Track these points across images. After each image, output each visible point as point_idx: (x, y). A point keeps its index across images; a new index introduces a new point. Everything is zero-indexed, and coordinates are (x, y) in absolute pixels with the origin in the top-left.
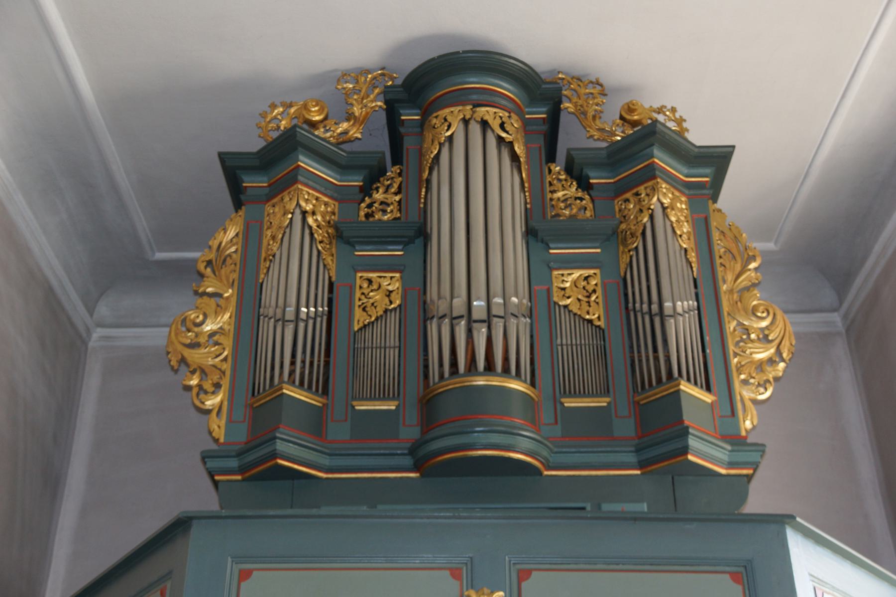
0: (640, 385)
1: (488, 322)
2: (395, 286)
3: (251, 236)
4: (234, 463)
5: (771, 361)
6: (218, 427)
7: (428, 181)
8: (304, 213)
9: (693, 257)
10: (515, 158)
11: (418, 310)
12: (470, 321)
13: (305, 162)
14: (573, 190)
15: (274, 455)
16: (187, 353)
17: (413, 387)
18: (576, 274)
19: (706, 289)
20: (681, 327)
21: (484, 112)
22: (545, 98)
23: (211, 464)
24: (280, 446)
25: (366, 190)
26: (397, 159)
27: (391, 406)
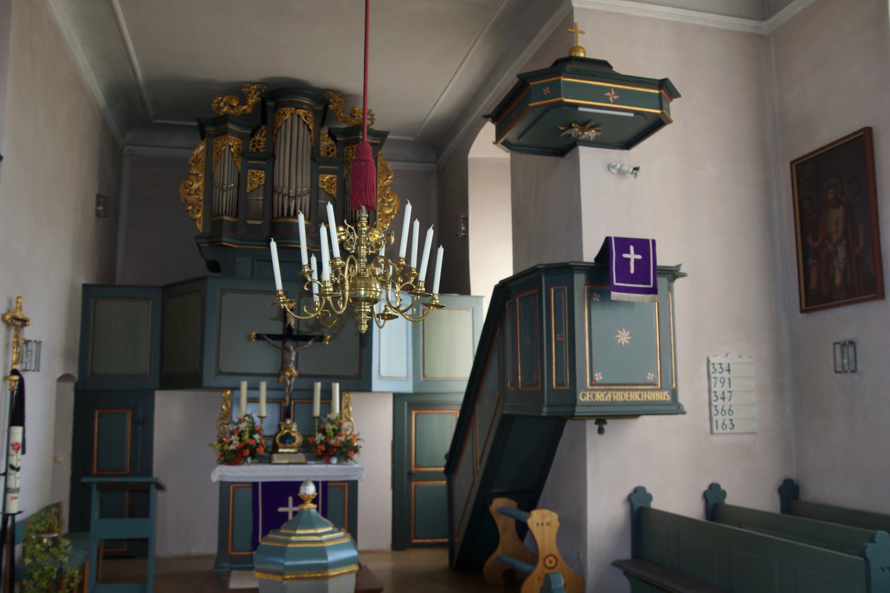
1: (295, 198)
2: (263, 175)
3: (209, 151)
4: (206, 241)
5: (391, 214)
6: (199, 226)
7: (276, 136)
8: (230, 147)
10: (309, 130)
11: (270, 188)
12: (289, 197)
13: (231, 126)
14: (331, 142)
15: (221, 241)
16: (188, 198)
18: (328, 177)
21: (301, 112)
22: (323, 103)
23: (199, 240)
24: (223, 239)
25: (252, 135)
26: (264, 121)
27: (259, 223)
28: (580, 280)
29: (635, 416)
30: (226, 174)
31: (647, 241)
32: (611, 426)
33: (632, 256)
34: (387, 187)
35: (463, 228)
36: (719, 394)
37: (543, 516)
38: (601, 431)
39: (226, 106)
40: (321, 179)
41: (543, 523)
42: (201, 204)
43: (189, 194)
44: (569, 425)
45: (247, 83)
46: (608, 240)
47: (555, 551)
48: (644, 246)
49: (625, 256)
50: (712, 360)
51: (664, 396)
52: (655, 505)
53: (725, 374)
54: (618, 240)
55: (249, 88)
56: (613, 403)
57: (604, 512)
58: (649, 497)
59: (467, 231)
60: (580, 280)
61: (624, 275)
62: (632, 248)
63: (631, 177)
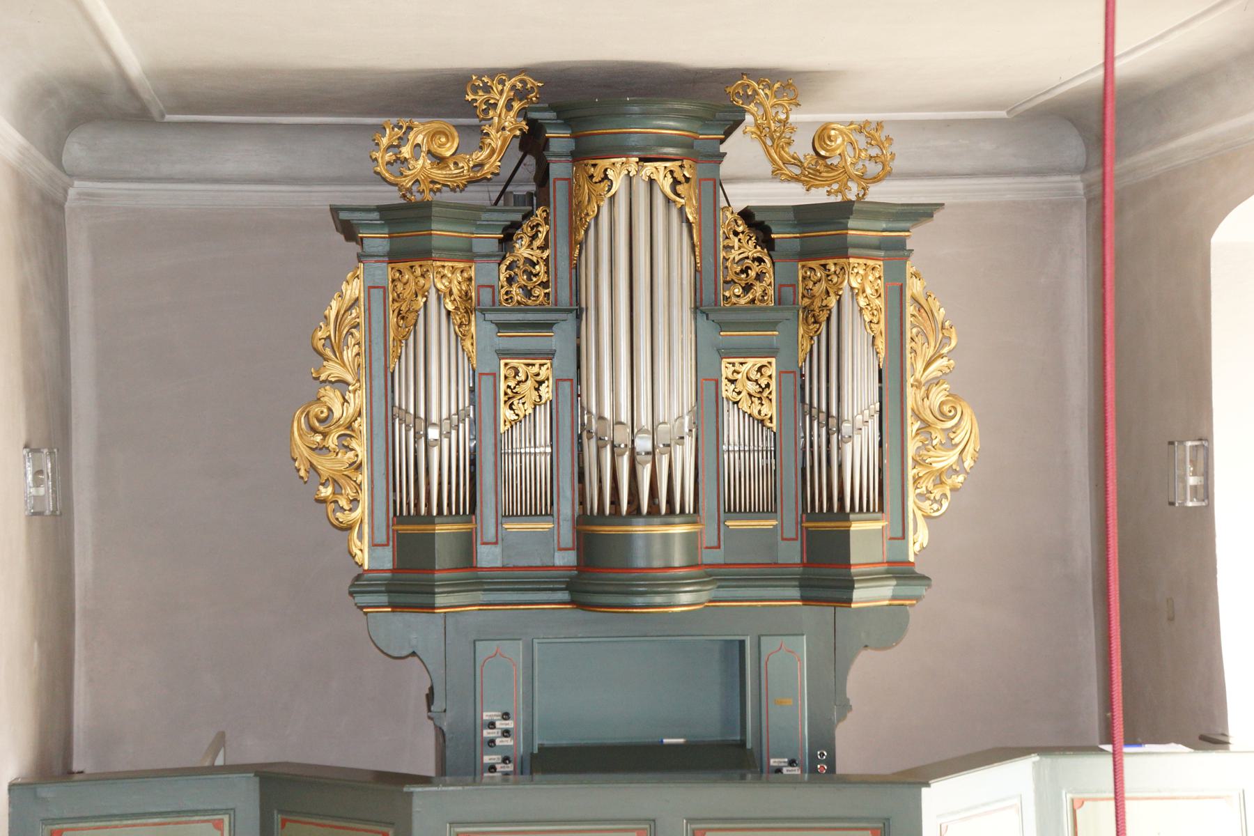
0: (809, 511)
4: (384, 599)
5: (953, 471)
6: (363, 554)
7: (582, 244)
9: (881, 344)
14: (752, 250)
16: (317, 460)
17: (566, 508)
18: (751, 361)
19: (891, 380)
20: (858, 451)
25: (507, 240)
30: (442, 393)
34: (937, 381)
35: (1192, 481)
39: (424, 155)
40: (727, 372)
42: (363, 477)
43: (321, 449)
45: (480, 73)
55: (487, 89)
59: (1206, 492)
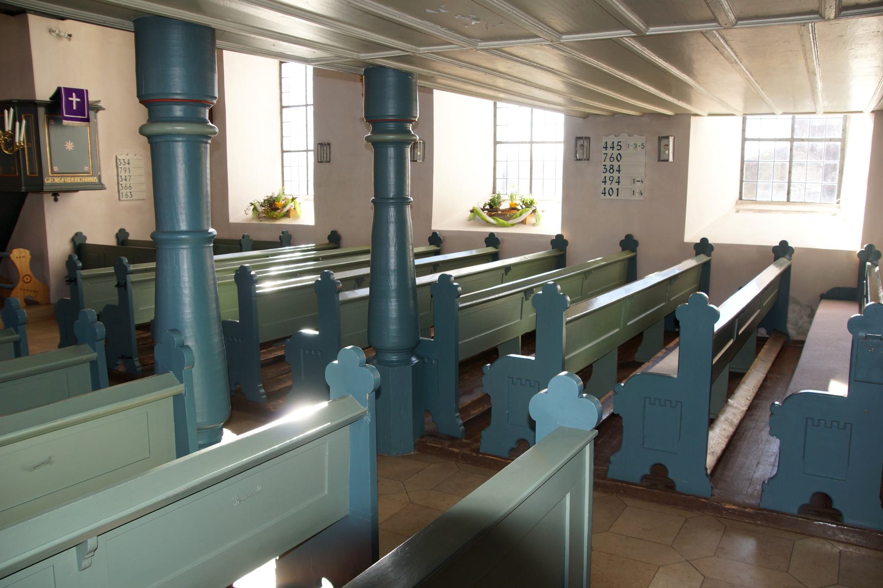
28: (41, 111)
29: (77, 191)
31: (83, 90)
32: (61, 197)
33: (75, 99)
36: (123, 178)
37: (20, 252)
38: (56, 200)
41: (20, 257)
44: (30, 199)
46: (59, 89)
47: (30, 273)
48: (81, 93)
49: (70, 99)
50: (119, 157)
51: (94, 179)
52: (89, 241)
53: (127, 166)
54: (65, 89)
56: (65, 184)
57: (58, 247)
58: (85, 238)
60: (41, 111)
61: (70, 110)
62: (74, 94)
63: (66, 40)
